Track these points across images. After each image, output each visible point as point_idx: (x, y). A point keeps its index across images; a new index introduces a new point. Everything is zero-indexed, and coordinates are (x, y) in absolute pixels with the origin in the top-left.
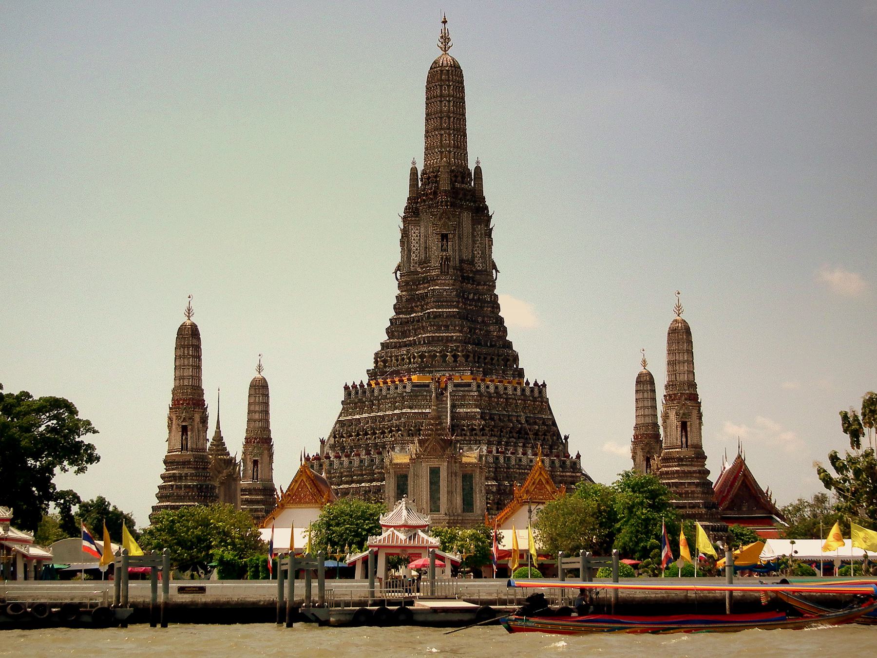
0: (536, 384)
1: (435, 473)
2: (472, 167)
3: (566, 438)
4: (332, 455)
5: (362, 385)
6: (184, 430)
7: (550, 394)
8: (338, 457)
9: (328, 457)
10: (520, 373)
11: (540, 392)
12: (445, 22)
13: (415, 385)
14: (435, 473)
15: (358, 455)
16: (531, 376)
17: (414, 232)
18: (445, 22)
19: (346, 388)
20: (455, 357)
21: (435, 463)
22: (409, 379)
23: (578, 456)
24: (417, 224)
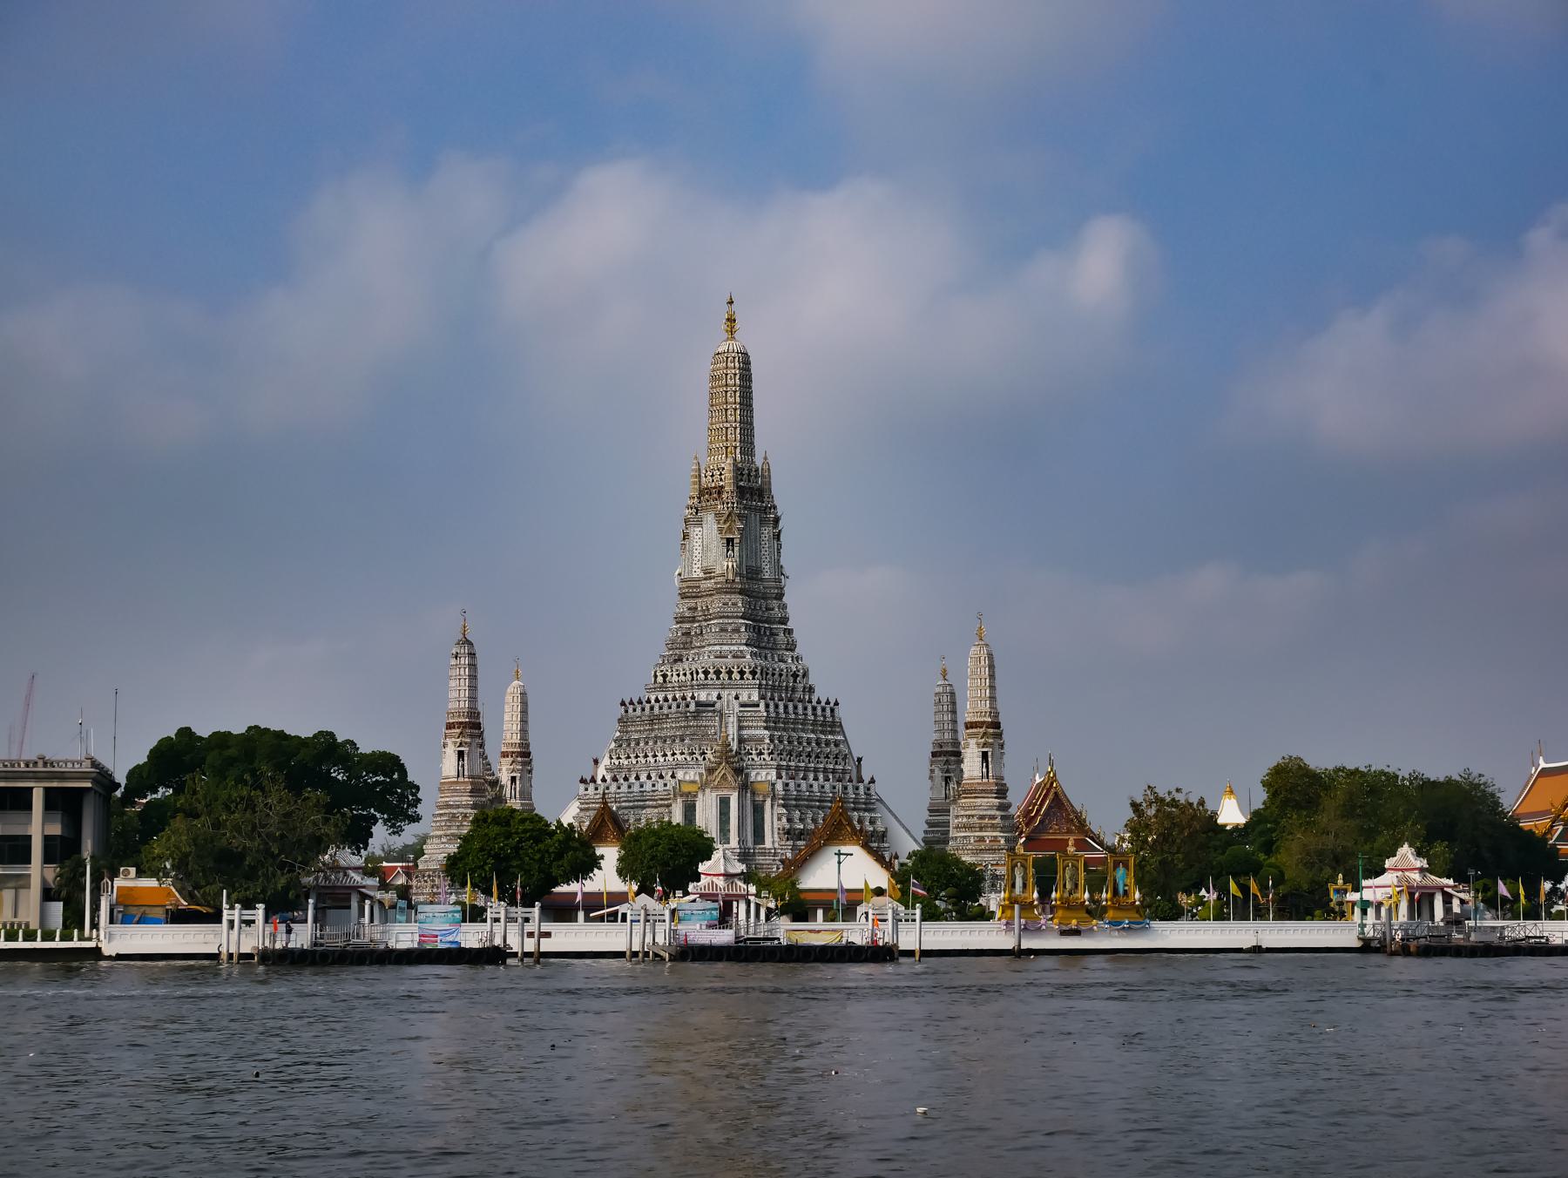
0: (828, 703)
1: (724, 803)
2: (758, 461)
3: (860, 760)
4: (608, 778)
5: (640, 702)
6: (461, 754)
7: (841, 713)
8: (615, 779)
9: (604, 780)
10: (811, 690)
11: (832, 710)
12: (731, 302)
13: (698, 704)
14: (724, 803)
15: (637, 778)
16: (821, 693)
17: (695, 532)
18: (731, 302)
19: (623, 704)
20: (742, 673)
21: (725, 793)
22: (693, 697)
23: (872, 781)
24: (700, 523)
